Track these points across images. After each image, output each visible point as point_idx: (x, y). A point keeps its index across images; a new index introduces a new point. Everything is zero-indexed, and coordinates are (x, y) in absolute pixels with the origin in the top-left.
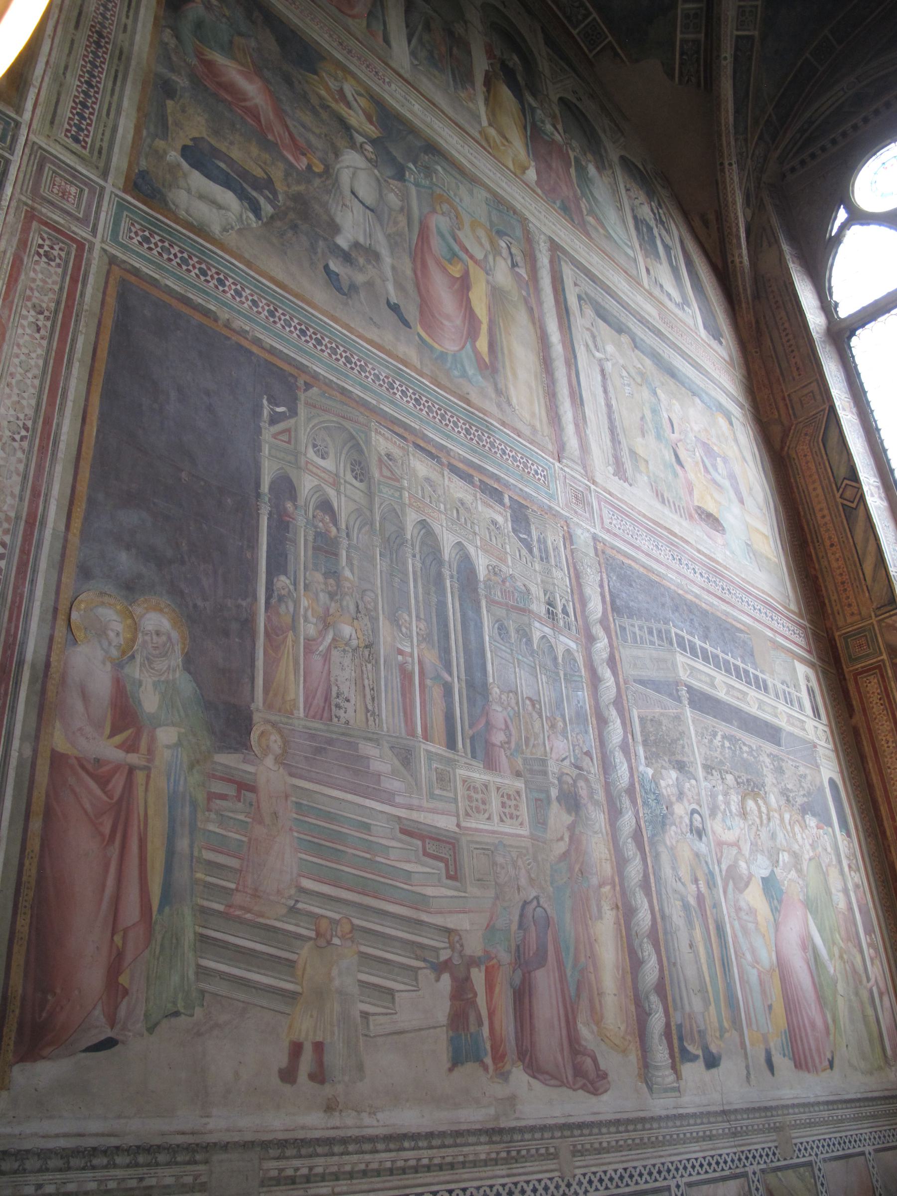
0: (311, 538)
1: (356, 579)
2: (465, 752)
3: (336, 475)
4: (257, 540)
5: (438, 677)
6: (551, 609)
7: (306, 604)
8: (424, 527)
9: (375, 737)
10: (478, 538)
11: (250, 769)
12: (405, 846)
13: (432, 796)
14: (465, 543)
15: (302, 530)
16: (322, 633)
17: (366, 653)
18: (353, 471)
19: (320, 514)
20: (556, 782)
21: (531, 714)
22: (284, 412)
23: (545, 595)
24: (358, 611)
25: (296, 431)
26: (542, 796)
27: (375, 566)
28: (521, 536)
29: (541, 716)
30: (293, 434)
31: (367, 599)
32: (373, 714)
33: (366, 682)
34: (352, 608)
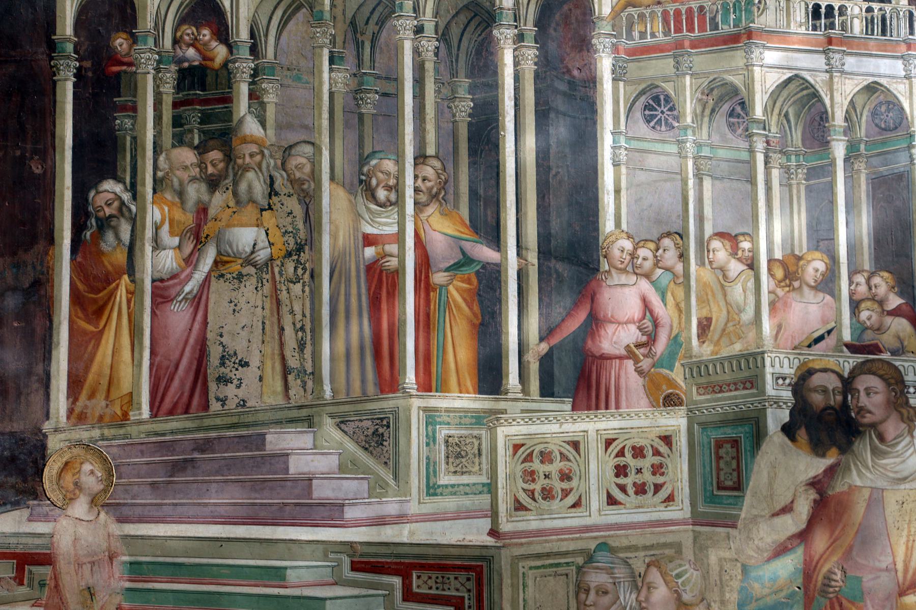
0: (168, 89)
1: (271, 132)
2: (525, 390)
4: (53, 135)
5: (466, 260)
7: (158, 217)
9: (304, 413)
11: (41, 527)
12: (364, 592)
13: (432, 490)
15: (150, 78)
16: (191, 261)
17: (290, 267)
19: (189, 30)
20: (787, 394)
21: (723, 270)
24: (272, 192)
26: (741, 432)
27: (316, 92)
29: (752, 265)
31: (300, 160)
32: (302, 372)
33: (287, 321)
34: (259, 189)
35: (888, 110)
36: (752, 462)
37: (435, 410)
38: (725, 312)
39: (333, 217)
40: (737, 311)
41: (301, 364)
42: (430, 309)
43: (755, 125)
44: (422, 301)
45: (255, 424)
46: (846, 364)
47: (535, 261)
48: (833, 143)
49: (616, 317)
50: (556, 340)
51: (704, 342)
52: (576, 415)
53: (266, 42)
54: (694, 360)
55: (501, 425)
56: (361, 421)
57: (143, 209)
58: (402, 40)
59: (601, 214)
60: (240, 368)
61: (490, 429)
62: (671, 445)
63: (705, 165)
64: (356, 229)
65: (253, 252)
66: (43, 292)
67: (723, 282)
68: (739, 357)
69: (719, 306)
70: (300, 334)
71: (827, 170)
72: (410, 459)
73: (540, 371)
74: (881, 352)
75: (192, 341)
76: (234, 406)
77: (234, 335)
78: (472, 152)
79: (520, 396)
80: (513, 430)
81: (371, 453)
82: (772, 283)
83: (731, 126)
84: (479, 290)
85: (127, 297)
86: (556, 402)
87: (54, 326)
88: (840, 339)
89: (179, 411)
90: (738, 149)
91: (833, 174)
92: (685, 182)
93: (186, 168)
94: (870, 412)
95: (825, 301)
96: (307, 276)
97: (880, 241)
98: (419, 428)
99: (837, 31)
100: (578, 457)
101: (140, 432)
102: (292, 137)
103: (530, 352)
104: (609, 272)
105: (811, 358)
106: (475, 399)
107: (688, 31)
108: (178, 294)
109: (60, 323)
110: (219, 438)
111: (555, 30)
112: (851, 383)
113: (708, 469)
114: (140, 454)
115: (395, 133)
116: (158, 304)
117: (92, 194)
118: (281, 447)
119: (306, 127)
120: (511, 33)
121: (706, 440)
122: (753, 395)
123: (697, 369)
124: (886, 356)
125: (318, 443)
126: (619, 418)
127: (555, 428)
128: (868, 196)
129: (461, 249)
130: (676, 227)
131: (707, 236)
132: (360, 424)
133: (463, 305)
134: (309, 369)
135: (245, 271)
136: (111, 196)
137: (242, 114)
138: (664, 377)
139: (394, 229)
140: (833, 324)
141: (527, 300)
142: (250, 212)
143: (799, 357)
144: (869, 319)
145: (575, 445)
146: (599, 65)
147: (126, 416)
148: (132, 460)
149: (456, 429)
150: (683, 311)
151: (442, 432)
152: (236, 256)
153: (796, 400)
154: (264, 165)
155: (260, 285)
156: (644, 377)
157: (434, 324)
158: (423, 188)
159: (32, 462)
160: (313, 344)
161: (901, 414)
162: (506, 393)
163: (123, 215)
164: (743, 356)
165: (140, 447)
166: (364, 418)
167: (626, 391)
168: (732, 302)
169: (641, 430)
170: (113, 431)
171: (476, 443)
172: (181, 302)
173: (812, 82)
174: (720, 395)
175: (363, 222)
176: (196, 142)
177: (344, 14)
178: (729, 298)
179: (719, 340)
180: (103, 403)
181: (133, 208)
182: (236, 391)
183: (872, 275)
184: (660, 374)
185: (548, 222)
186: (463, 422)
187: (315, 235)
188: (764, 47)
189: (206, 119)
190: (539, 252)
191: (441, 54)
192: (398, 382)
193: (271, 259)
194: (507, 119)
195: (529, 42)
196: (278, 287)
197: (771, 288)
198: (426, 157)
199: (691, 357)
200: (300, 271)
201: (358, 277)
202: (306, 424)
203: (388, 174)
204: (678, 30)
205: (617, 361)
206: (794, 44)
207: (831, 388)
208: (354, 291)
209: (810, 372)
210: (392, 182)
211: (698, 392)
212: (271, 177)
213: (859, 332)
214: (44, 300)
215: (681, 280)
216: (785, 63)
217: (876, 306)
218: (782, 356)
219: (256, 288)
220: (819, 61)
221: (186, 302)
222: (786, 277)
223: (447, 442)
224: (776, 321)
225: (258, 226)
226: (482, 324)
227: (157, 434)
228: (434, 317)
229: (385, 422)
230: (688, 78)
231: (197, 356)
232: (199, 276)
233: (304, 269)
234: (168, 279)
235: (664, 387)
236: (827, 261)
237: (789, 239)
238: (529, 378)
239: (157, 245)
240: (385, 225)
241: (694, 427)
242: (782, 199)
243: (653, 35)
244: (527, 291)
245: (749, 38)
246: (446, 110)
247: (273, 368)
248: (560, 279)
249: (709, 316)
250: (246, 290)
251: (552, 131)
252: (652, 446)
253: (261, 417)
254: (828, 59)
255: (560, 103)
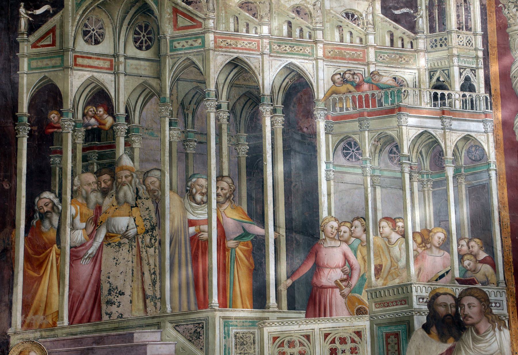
0: (80, 141)
1: (137, 164)
2: (279, 306)
3: (114, 56)
4: (16, 168)
5: (246, 234)
6: (439, 92)
7: (74, 211)
8: (236, 66)
9: (155, 321)
10: (321, 45)
14: (297, 61)
15: (70, 135)
16: (92, 236)
17: (148, 238)
18: (135, 41)
19: (91, 109)
20: (425, 307)
21: (388, 238)
22: (47, 12)
23: (431, 78)
24: (138, 197)
25: (62, 26)
26: (400, 329)
28: (397, 12)
29: (404, 235)
30: (58, 32)
31: (153, 179)
32: (154, 298)
33: (146, 269)
34: (130, 195)
35: (476, 150)
36: (406, 346)
37: (229, 318)
38: (389, 261)
39: (172, 210)
40: (396, 261)
41: (154, 293)
42: (226, 261)
43: (404, 158)
44: (221, 257)
45: (128, 328)
46: (457, 290)
47: (284, 234)
48: (447, 168)
49: (329, 265)
50: (296, 278)
51: (378, 278)
52: (308, 320)
53: (134, 115)
54: (373, 288)
55: (266, 326)
56: (187, 325)
57: (65, 208)
58: (209, 112)
59: (320, 207)
60: (119, 296)
61: (260, 328)
62: (361, 337)
63: (377, 180)
64: (185, 217)
65: (127, 231)
66: (9, 255)
67: (388, 245)
68: (398, 287)
69: (386, 258)
70: (153, 276)
71: (443, 182)
72: (215, 346)
73: (287, 295)
74: (476, 283)
75: (92, 281)
76: (116, 317)
77: (116, 277)
78: (249, 174)
79: (277, 309)
80: (273, 329)
81: (193, 343)
82: (415, 245)
83: (391, 159)
84: (253, 250)
85: (56, 257)
86: (297, 313)
87: (15, 274)
88: (453, 276)
89: (85, 321)
90: (395, 171)
91: (447, 185)
92: (366, 189)
93: (89, 184)
94: (471, 317)
95: (444, 255)
96: (157, 244)
97: (473, 221)
98: (220, 328)
99: (447, 107)
100: (309, 344)
101: (63, 333)
102: (149, 167)
103: (282, 285)
104: (325, 239)
105: (437, 287)
106: (251, 312)
107: (366, 107)
108: (85, 255)
109: (18, 273)
110: (107, 336)
111: (293, 107)
112: (460, 301)
113: (382, 350)
114: (62, 346)
115: (206, 164)
116: (74, 261)
117: (37, 199)
118: (142, 340)
119: (156, 161)
120: (269, 108)
121: (380, 334)
122: (406, 308)
123: (375, 293)
124: (479, 286)
125: (163, 338)
126: (332, 321)
127: (296, 327)
128: (466, 197)
129: (243, 227)
130: (362, 214)
131: (379, 219)
132: (187, 327)
133: (244, 259)
134: (158, 297)
135: (122, 241)
136: (48, 201)
137: (121, 154)
138: (356, 298)
139: (206, 217)
140: (449, 268)
141: (280, 256)
142: (125, 208)
143: (431, 286)
144: (469, 265)
145: (308, 337)
146: (318, 126)
147: (55, 324)
148: (58, 349)
149: (241, 329)
150: (366, 261)
151: (233, 331)
152: (118, 233)
153: (429, 311)
154: (133, 182)
155: (131, 249)
156: (346, 298)
157: (228, 270)
158: (222, 194)
159: (1, 352)
160: (161, 282)
161: (488, 318)
162: (269, 308)
163: (54, 211)
164: (400, 286)
165: (62, 342)
166: (189, 323)
167: (336, 306)
168: (394, 256)
169: (344, 328)
170: (48, 333)
171: (252, 337)
172: (86, 259)
173: (435, 135)
174: (388, 308)
175: (188, 213)
176: (95, 170)
177: (177, 99)
178: (391, 253)
179: (386, 277)
180: (42, 317)
181: (60, 207)
182: (117, 309)
183: (470, 240)
184: (354, 296)
185: (291, 212)
186: (244, 325)
187: (162, 221)
188: (408, 116)
189: (101, 157)
190: (286, 229)
191: (230, 120)
192: (208, 303)
193: (137, 234)
194: (268, 156)
195: (279, 113)
196: (141, 250)
197: (415, 248)
198: (223, 177)
199: (371, 287)
200: (153, 241)
201: (186, 244)
202: (156, 327)
203: (202, 186)
204: (361, 106)
205: (330, 289)
206: (424, 114)
207: (449, 304)
208: (183, 252)
209: (437, 295)
210: (204, 191)
211: (375, 307)
212: (137, 189)
213: (464, 272)
214: (9, 260)
215: (365, 244)
216: (419, 125)
217: (472, 258)
218: (421, 286)
219: (129, 251)
220: (438, 123)
221: (89, 259)
222: (423, 242)
223: (236, 336)
224: (418, 266)
225: (129, 216)
226: (255, 269)
227: (72, 334)
228: (228, 266)
229: (201, 325)
230: (367, 132)
231: (95, 290)
232: (96, 245)
233: (156, 240)
234: (79, 247)
235: (357, 304)
236: (445, 233)
237: (424, 220)
238: (281, 299)
239: (73, 228)
240: (201, 214)
241: (373, 326)
242: (419, 199)
243: (347, 109)
244: (280, 251)
245: (400, 110)
246: (234, 151)
247: (138, 295)
248: (298, 244)
249: (381, 264)
250: (123, 252)
251: (293, 162)
252: (350, 337)
253: (131, 323)
254: (443, 122)
255: (296, 146)
